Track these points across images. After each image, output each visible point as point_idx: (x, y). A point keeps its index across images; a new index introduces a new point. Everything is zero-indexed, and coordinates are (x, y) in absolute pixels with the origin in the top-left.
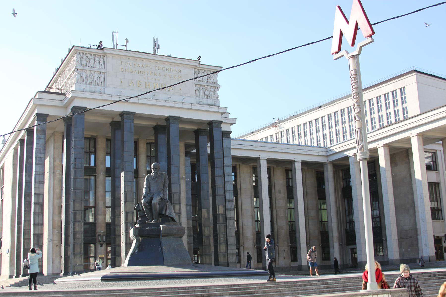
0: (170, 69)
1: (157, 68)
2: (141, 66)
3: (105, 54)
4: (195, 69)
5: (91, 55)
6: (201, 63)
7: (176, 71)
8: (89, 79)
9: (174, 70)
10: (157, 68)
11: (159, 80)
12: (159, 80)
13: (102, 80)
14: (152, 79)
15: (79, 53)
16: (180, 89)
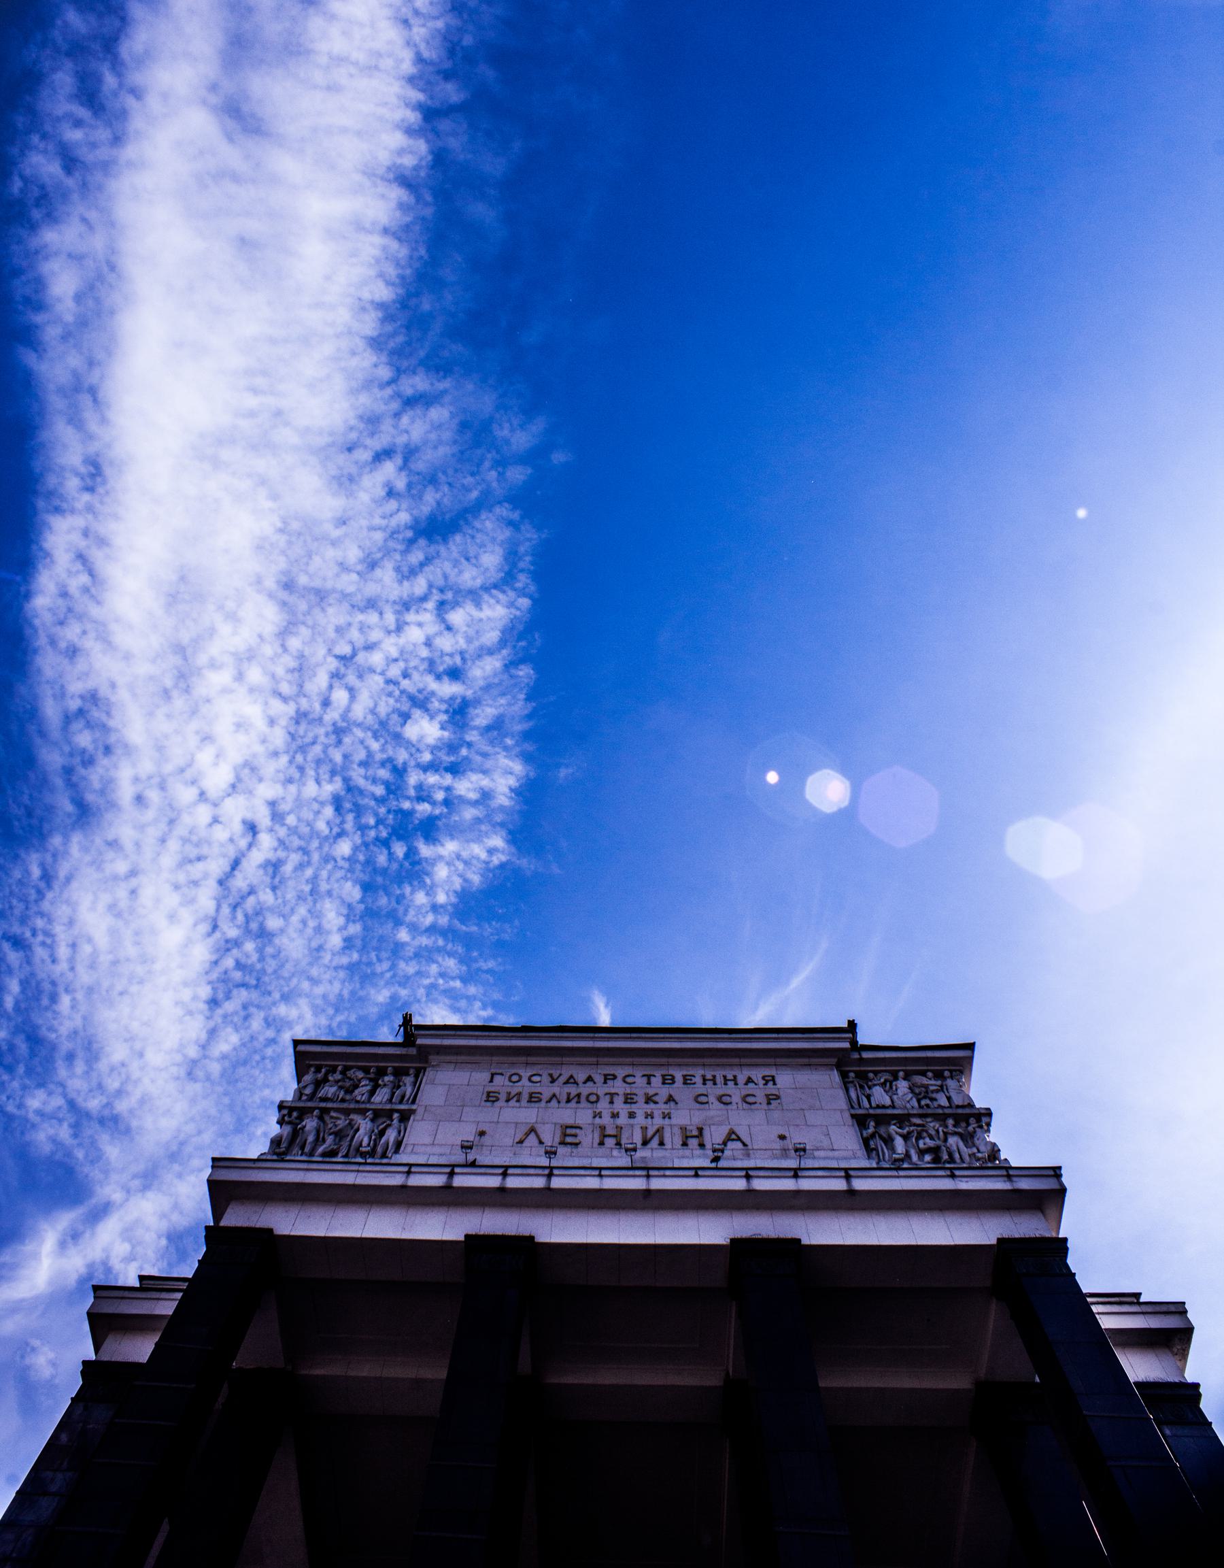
0: (719, 1080)
1: (657, 1081)
2: (581, 1076)
3: (425, 1054)
4: (844, 1075)
5: (366, 1070)
6: (863, 1039)
7: (749, 1080)
8: (330, 1140)
9: (742, 1079)
10: (657, 1081)
11: (667, 1116)
12: (667, 1116)
13: (391, 1135)
14: (632, 1115)
15: (318, 1070)
16: (782, 1137)
